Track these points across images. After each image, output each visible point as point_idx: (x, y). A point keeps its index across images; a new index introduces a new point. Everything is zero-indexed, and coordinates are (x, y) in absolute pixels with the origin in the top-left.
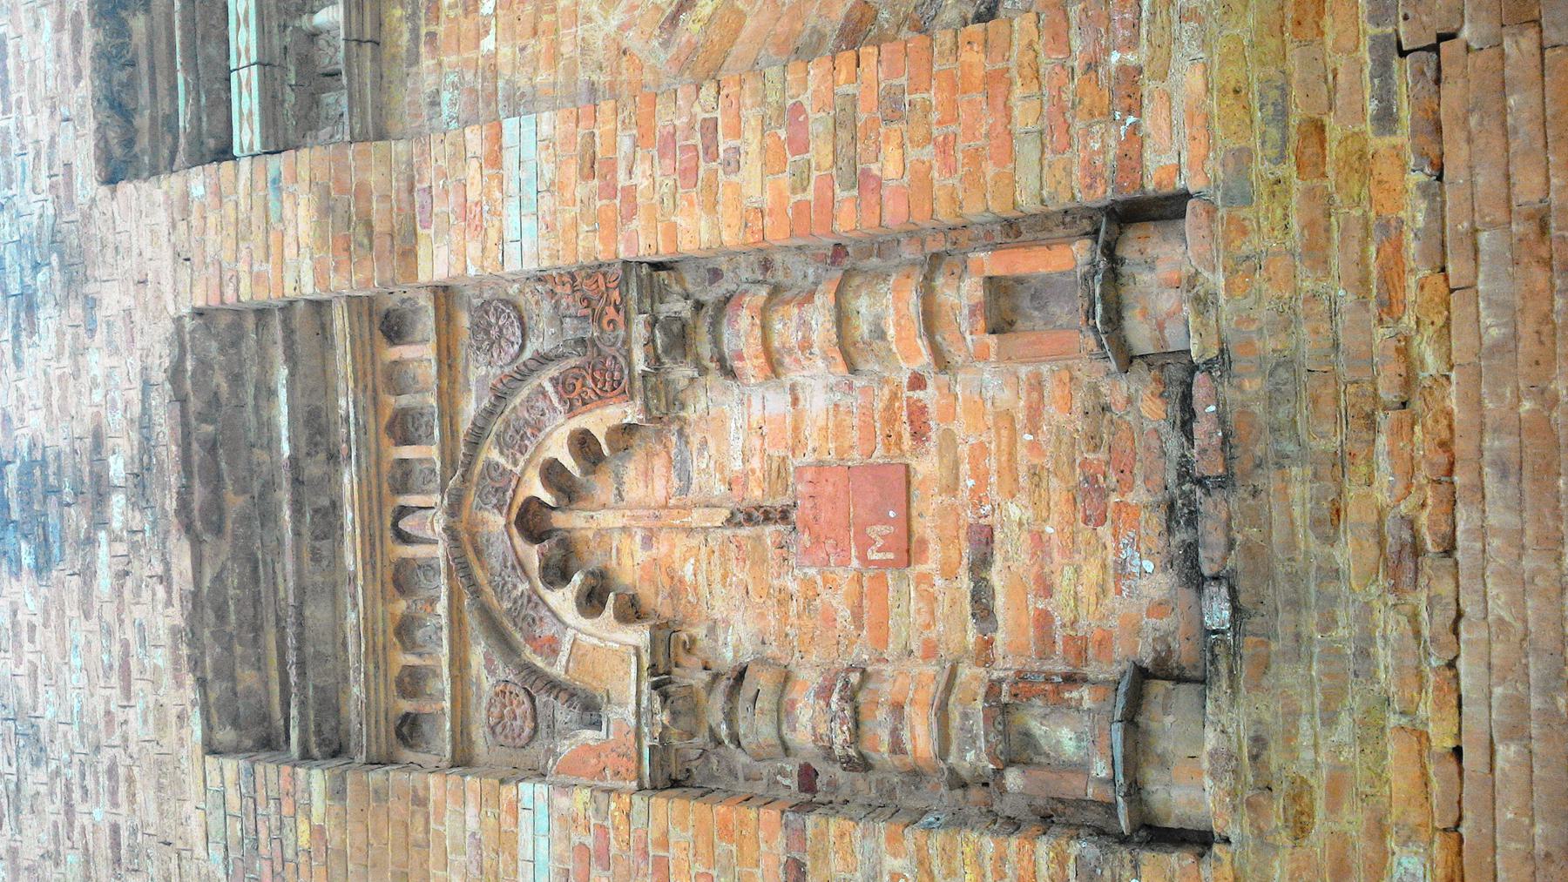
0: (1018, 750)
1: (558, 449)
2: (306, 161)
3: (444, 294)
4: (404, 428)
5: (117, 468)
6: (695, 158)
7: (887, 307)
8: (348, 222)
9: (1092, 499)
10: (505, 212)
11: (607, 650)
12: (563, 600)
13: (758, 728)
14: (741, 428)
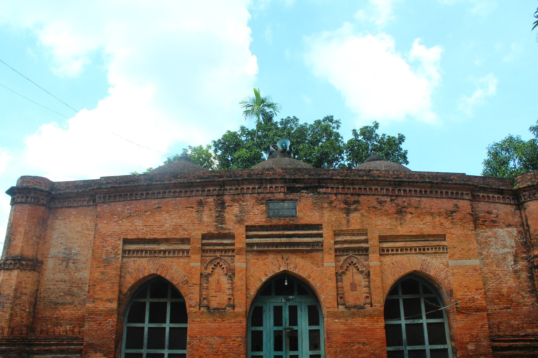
0: (204, 299)
1: (223, 266)
2: (244, 246)
3: (234, 256)
5: (223, 226)
8: (240, 249)
9: (219, 304)
10: (239, 263)
12: (213, 266)
14: (224, 280)
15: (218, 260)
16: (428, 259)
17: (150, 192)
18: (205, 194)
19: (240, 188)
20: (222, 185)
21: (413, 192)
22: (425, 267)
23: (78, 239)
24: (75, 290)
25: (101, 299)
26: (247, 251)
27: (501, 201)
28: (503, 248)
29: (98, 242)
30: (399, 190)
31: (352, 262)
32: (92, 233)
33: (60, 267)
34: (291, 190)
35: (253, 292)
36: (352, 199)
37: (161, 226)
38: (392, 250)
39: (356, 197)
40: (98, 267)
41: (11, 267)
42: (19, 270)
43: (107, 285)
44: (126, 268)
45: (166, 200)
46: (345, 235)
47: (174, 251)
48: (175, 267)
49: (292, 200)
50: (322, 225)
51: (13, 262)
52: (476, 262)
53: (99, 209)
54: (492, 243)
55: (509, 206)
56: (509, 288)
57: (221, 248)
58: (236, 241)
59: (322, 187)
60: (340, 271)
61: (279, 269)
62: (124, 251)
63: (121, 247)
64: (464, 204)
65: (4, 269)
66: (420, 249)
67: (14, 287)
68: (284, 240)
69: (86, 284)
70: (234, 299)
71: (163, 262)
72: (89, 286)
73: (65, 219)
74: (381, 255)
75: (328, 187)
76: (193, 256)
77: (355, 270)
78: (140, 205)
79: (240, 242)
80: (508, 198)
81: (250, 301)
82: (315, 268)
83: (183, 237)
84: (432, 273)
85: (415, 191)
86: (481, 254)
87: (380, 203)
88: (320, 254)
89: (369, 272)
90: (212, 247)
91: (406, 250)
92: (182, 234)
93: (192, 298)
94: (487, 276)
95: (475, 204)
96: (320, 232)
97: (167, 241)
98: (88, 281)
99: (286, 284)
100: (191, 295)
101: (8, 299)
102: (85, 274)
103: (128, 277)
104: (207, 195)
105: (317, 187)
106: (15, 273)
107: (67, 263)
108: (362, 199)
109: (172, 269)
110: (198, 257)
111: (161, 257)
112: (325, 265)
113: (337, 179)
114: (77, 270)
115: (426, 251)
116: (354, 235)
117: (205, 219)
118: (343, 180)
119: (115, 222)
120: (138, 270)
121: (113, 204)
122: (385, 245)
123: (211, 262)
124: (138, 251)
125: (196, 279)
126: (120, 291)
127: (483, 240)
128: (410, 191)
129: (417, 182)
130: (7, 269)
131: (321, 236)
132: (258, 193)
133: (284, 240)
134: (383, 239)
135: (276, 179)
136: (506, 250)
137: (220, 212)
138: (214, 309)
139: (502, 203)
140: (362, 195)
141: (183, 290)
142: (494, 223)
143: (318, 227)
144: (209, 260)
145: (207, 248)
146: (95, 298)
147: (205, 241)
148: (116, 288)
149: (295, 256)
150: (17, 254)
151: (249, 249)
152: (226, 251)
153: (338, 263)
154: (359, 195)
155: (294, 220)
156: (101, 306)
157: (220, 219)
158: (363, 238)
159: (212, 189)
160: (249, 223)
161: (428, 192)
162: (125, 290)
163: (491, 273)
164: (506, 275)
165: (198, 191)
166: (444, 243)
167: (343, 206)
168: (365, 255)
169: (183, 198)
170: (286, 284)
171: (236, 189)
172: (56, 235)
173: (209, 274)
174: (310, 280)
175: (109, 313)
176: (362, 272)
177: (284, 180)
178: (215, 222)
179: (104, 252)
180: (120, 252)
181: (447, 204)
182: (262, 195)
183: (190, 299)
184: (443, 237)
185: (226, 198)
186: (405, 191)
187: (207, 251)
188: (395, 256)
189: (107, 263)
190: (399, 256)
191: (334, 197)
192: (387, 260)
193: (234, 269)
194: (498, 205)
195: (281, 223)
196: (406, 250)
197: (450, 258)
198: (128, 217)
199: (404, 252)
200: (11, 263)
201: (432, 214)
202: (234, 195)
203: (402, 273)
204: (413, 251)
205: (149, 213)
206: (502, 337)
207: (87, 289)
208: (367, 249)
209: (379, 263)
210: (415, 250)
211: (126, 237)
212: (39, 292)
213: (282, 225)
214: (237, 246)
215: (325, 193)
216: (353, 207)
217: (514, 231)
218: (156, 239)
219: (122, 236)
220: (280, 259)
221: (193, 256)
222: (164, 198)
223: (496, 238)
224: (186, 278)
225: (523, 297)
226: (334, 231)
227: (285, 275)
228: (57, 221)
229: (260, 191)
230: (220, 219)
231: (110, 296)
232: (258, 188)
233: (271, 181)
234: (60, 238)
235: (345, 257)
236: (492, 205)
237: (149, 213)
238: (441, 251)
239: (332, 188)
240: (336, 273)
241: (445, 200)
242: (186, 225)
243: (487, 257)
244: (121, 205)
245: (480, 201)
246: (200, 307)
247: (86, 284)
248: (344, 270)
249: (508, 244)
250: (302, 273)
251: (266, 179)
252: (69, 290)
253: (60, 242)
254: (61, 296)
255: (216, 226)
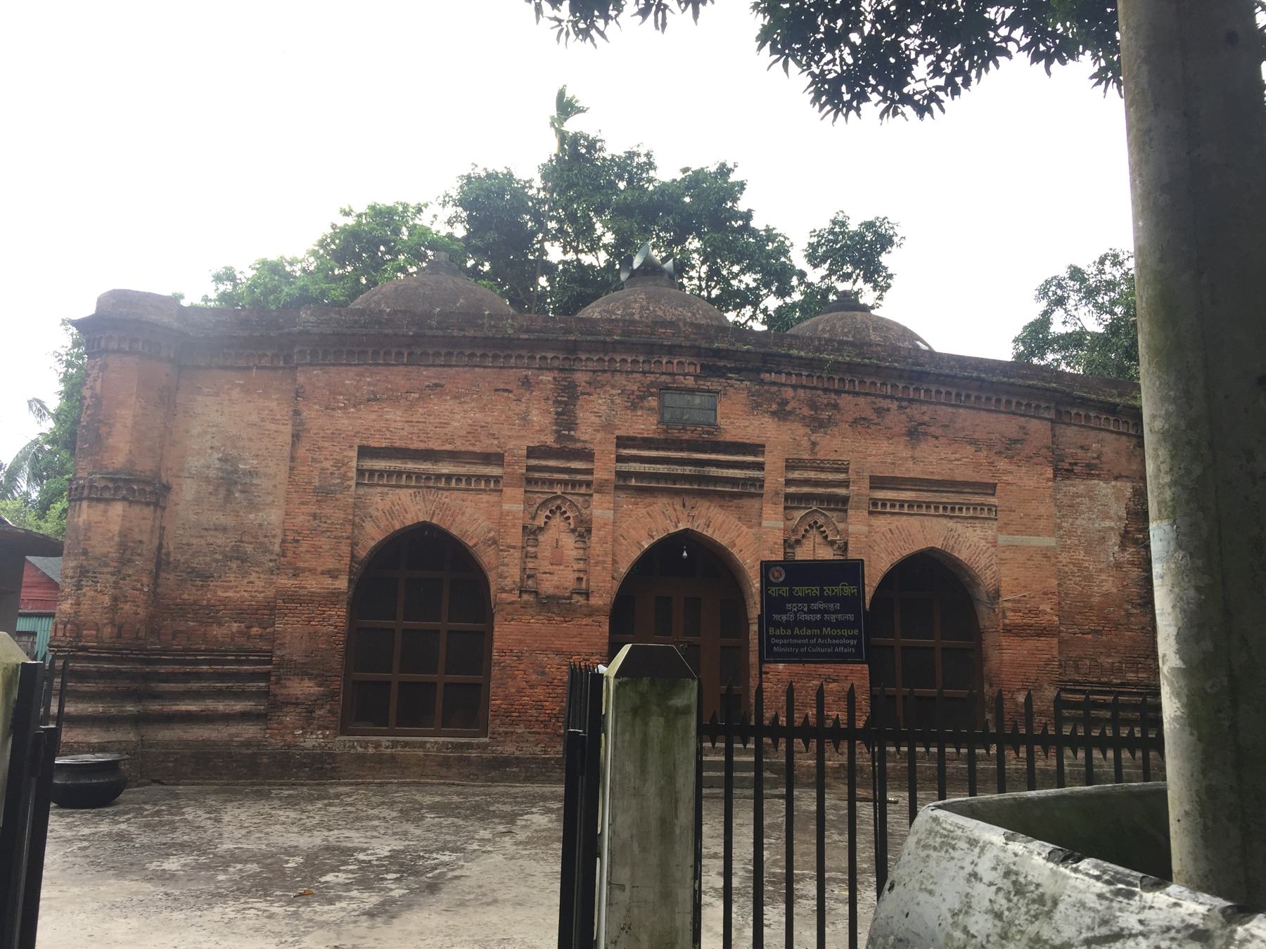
0: (529, 577)
2: (612, 477)
3: (591, 495)
4: (573, 486)
6: (603, 541)
7: (581, 565)
10: (601, 510)
11: (540, 521)
13: (531, 542)
14: (569, 541)
15: (559, 502)
16: (959, 527)
17: (419, 351)
18: (537, 363)
19: (607, 358)
20: (572, 349)
21: (943, 396)
22: (951, 542)
23: (250, 440)
24: (249, 549)
25: (312, 571)
26: (617, 488)
27: (1111, 428)
28: (1103, 520)
29: (303, 450)
30: (917, 390)
31: (816, 523)
32: (288, 429)
33: (213, 499)
34: (710, 371)
35: (624, 569)
36: (823, 399)
37: (444, 425)
38: (893, 506)
39: (833, 396)
40: (303, 503)
41: (107, 495)
42: (126, 504)
43: (325, 543)
44: (365, 508)
45: (453, 371)
46: (805, 468)
47: (469, 478)
48: (469, 511)
49: (709, 391)
50: (763, 446)
51: (111, 485)
52: (1050, 541)
53: (301, 379)
54: (1083, 507)
55: (1124, 438)
56: (1106, 595)
57: (566, 477)
58: (597, 464)
59: (770, 372)
60: (793, 538)
61: (676, 526)
62: (361, 472)
63: (354, 464)
64: (1038, 429)
65: (90, 499)
66: (945, 508)
67: (117, 539)
68: (688, 470)
69: (274, 536)
70: (588, 580)
71: (447, 500)
72: (284, 541)
73: (217, 395)
74: (871, 513)
75: (779, 372)
76: (508, 491)
77: (819, 539)
78: (397, 377)
79: (604, 469)
80: (1126, 422)
81: (616, 585)
82: (744, 528)
83: (490, 450)
84: (963, 555)
85: (949, 393)
86: (1060, 528)
87: (880, 411)
88: (755, 503)
89: (846, 544)
90: (546, 475)
91: (919, 506)
92: (486, 445)
93: (504, 574)
94: (1066, 569)
95: (1061, 429)
96: (760, 459)
97: (454, 456)
98: (279, 532)
99: (685, 554)
100: (505, 569)
101: (106, 565)
102: (273, 516)
103: (369, 526)
104: (540, 369)
105: (758, 371)
106: (118, 509)
107: (228, 490)
108: (845, 401)
109: (463, 514)
110: (519, 493)
111: (439, 489)
112: (765, 523)
113: (801, 358)
114: (253, 506)
115: (957, 513)
116: (822, 470)
117: (535, 416)
118: (812, 359)
119: (340, 408)
120: (391, 512)
121: (333, 370)
122: (880, 494)
123: (544, 504)
124: (390, 473)
125: (515, 536)
126: (353, 556)
127: (1066, 501)
128: (938, 392)
129: (955, 377)
130: (99, 500)
131: (760, 467)
132: (644, 373)
133: (688, 470)
134: (878, 482)
135: (681, 347)
136: (1108, 523)
137: (566, 404)
138: (548, 597)
139: (1112, 432)
140: (845, 392)
141: (487, 557)
142: (1091, 471)
143: (757, 449)
144: (539, 501)
145: (536, 475)
146: (297, 569)
147: (533, 462)
148: (345, 549)
149: (707, 504)
150: (118, 466)
151: (621, 483)
152: (574, 484)
153: (788, 523)
154: (838, 392)
155: (712, 433)
156: (313, 584)
157: (565, 421)
158: (842, 476)
159: (550, 355)
160: (622, 432)
161: (973, 398)
162: (362, 553)
163: (1074, 564)
164: (1101, 570)
165: (520, 357)
166: (992, 500)
167: (806, 411)
168: (840, 510)
169: (489, 370)
170: (685, 554)
171: (600, 360)
172: (199, 429)
173: (540, 529)
174: (734, 551)
175: (332, 597)
176: (832, 543)
177: (697, 351)
178: (557, 424)
179: (316, 472)
180: (353, 474)
181: (1006, 425)
182: (651, 378)
183: (501, 576)
184: (990, 489)
185: (581, 378)
186: (927, 391)
187: (536, 481)
188: (897, 517)
189: (325, 493)
190: (904, 518)
191: (789, 393)
192: (881, 523)
193: (591, 521)
194: (1103, 434)
195: (686, 437)
196: (919, 506)
197: (1000, 529)
198: (369, 400)
199: (915, 510)
200: (106, 488)
201: (973, 442)
202: (594, 372)
203: (906, 553)
204: (932, 511)
205: (417, 395)
206: (1080, 684)
207: (277, 548)
208: (845, 500)
209: (865, 529)
210: (936, 508)
211: (365, 443)
212: (164, 551)
213: (688, 441)
214: (599, 475)
215: (774, 383)
216: (825, 415)
217: (1127, 488)
218: (432, 450)
219: (357, 442)
220: (678, 507)
221: (508, 491)
222: (450, 366)
223: (1091, 498)
224: (492, 534)
225: (1129, 615)
226: (787, 460)
227: (686, 538)
228: (199, 398)
229: (647, 367)
230: (565, 421)
231: (331, 564)
232: (644, 362)
233: (672, 350)
234: (209, 437)
235: (803, 513)
236: (1092, 433)
237: (417, 395)
238: (985, 514)
239: (789, 374)
240: (785, 541)
241: (1002, 417)
242: (495, 426)
243: (1070, 534)
244: (351, 374)
245: (1069, 424)
246: (521, 592)
247: (274, 536)
248: (799, 537)
249: (1112, 512)
250: (722, 538)
251: (662, 346)
252: (236, 549)
253: (209, 444)
254: (217, 561)
255: (557, 432)
